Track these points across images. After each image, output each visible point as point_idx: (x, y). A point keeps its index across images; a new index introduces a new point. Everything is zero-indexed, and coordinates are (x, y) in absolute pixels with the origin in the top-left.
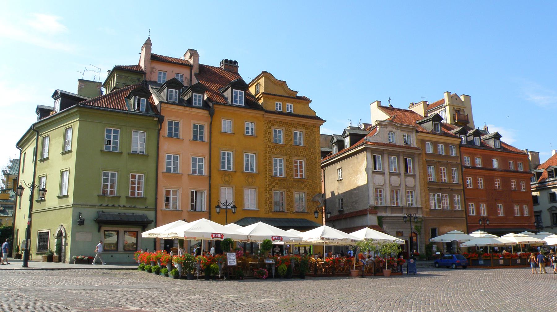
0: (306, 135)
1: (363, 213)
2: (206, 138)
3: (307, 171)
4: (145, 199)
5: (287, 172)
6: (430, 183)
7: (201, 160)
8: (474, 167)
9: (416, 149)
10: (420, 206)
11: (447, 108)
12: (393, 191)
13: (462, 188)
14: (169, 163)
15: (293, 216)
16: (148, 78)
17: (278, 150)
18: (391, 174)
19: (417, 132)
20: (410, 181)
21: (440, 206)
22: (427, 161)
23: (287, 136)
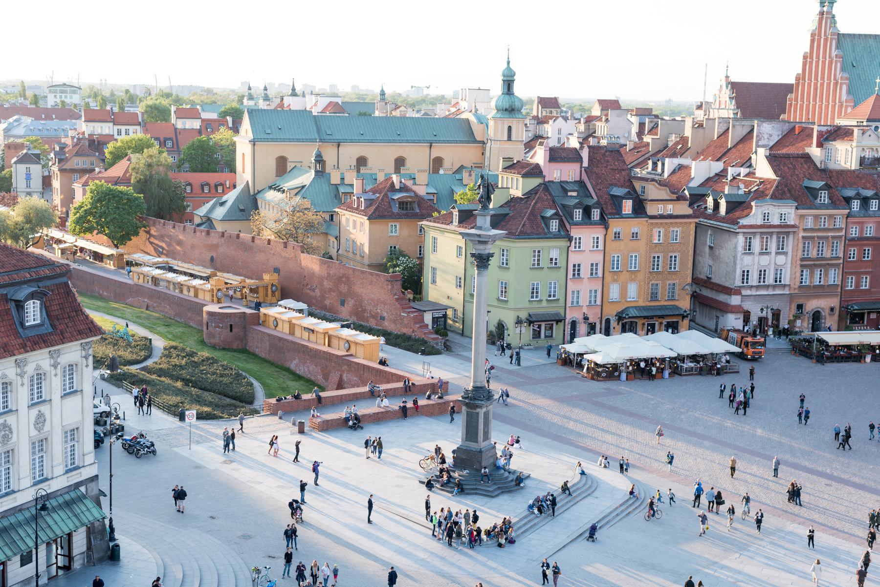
0: (682, 232)
1: (728, 291)
2: (601, 247)
3: (680, 264)
4: (558, 300)
5: (663, 267)
6: (802, 260)
7: (597, 265)
8: (861, 239)
9: (793, 226)
10: (788, 283)
11: (855, 150)
12: (761, 271)
13: (841, 261)
14: (574, 270)
15: (666, 303)
16: (547, 180)
17: (657, 249)
18: (761, 254)
19: (797, 208)
20: (781, 259)
21: (811, 282)
22: (803, 237)
23: (665, 235)
